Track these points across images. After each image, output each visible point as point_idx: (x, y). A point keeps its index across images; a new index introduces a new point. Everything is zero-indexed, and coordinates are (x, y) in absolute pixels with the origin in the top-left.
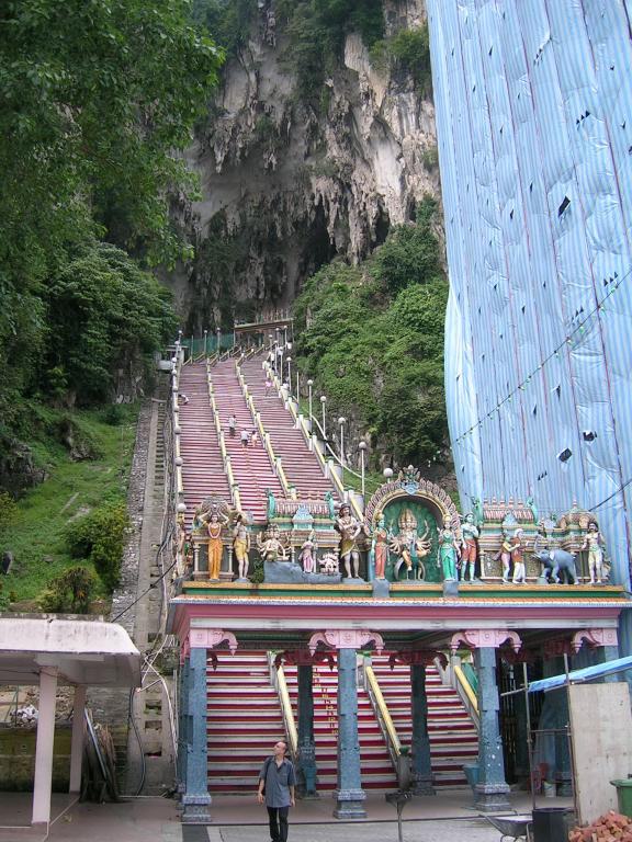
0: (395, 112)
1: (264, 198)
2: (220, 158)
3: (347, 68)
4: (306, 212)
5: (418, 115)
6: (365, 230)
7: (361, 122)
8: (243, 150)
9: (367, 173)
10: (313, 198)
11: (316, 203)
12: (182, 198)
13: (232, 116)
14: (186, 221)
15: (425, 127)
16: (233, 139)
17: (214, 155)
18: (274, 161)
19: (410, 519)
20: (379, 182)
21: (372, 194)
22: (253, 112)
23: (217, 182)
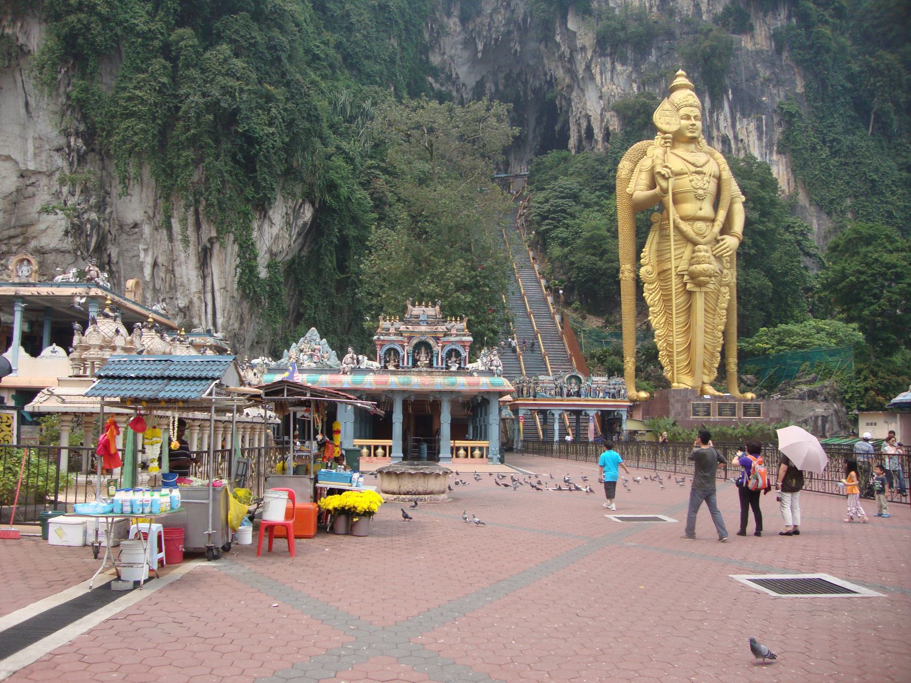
0: (598, 70)
1: (511, 71)
2: (480, 47)
3: (568, 30)
4: (541, 84)
5: (612, 72)
6: (579, 131)
7: (578, 65)
8: (497, 40)
9: (581, 95)
10: (546, 74)
11: (548, 78)
12: (454, 76)
13: (489, 12)
14: (457, 91)
15: (616, 81)
16: (490, 30)
17: (476, 44)
18: (519, 49)
19: (573, 381)
20: (588, 106)
21: (583, 113)
22: (503, 11)
23: (474, 61)
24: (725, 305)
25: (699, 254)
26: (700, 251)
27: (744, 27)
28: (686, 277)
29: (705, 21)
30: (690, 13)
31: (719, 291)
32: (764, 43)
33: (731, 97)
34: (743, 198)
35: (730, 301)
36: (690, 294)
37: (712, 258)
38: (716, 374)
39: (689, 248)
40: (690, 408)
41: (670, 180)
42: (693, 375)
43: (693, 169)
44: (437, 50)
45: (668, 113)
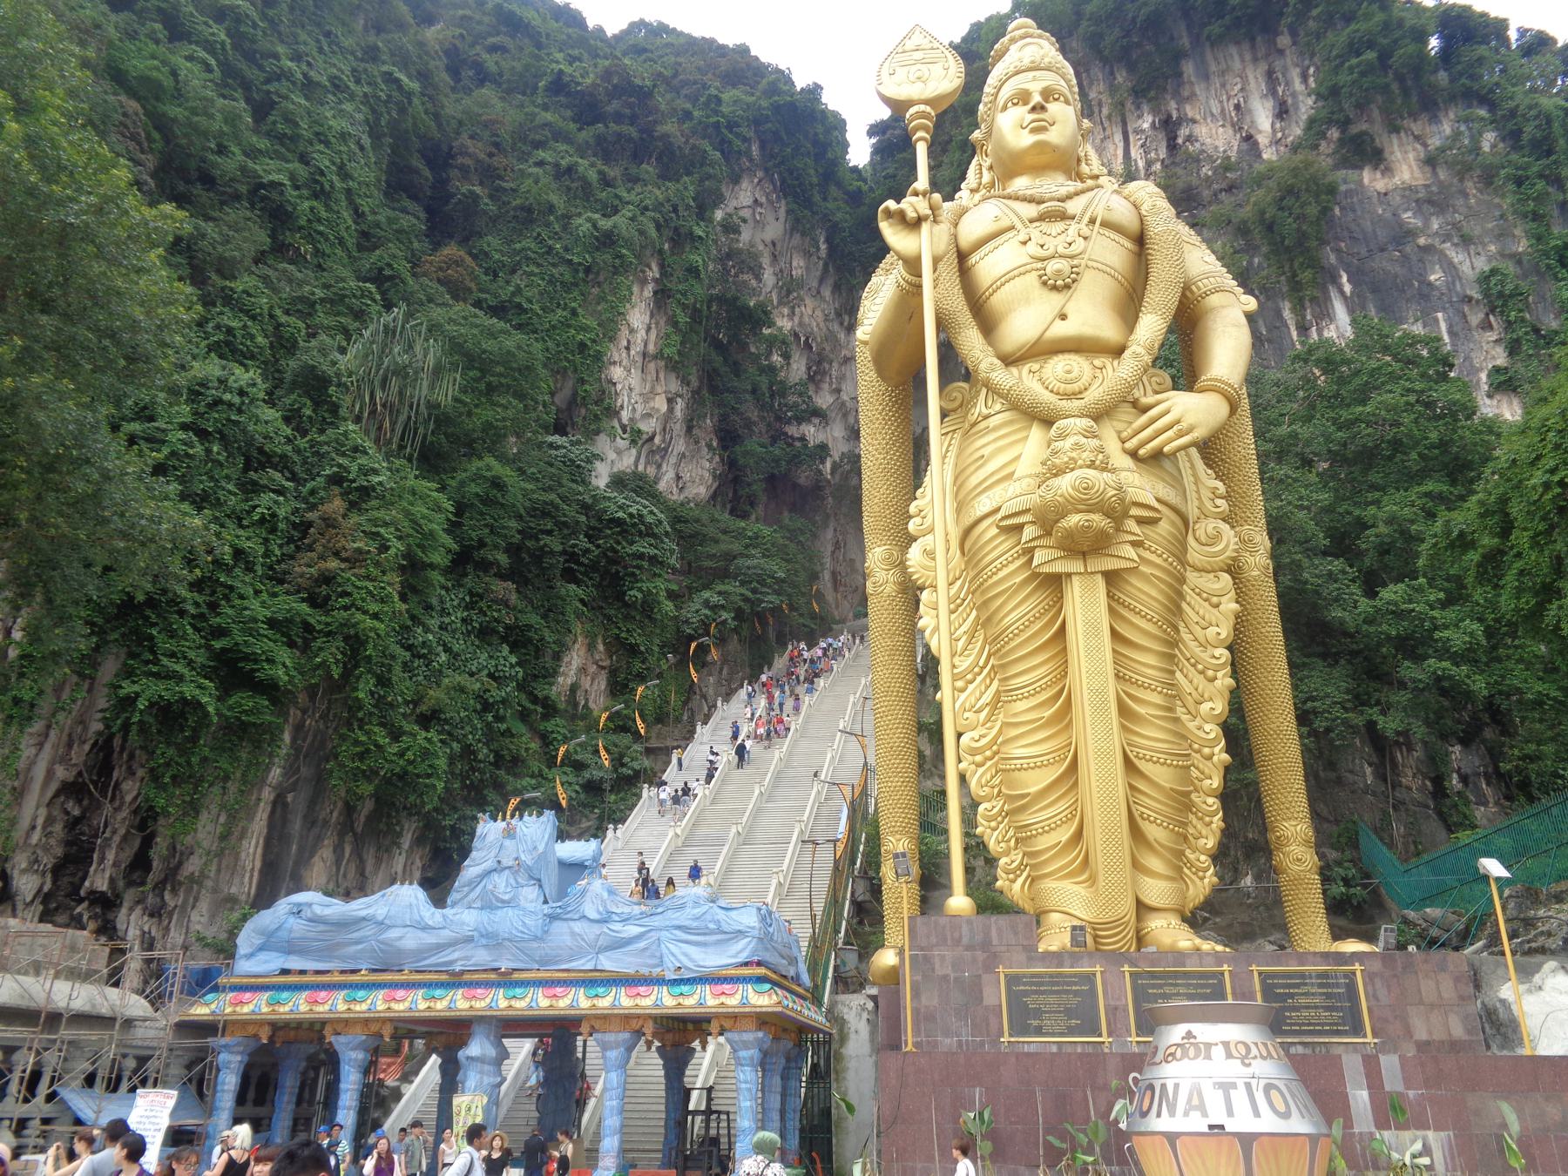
24: (1225, 631)
25: (1059, 444)
26: (1062, 436)
27: (1364, 152)
28: (1029, 532)
29: (1270, 162)
30: (1233, 154)
31: (1182, 580)
32: (1417, 173)
33: (1348, 288)
34: (1251, 303)
35: (1241, 623)
36: (1054, 584)
37: (1122, 461)
38: (1210, 878)
39: (1036, 433)
40: (997, 994)
41: (925, 227)
42: (1092, 880)
43: (1032, 210)
44: (826, 386)
45: (918, 55)
